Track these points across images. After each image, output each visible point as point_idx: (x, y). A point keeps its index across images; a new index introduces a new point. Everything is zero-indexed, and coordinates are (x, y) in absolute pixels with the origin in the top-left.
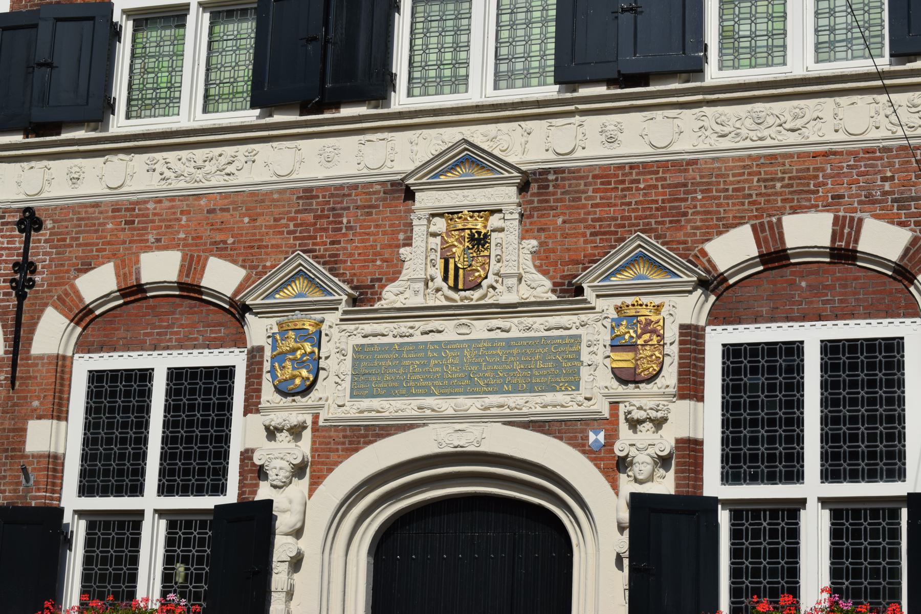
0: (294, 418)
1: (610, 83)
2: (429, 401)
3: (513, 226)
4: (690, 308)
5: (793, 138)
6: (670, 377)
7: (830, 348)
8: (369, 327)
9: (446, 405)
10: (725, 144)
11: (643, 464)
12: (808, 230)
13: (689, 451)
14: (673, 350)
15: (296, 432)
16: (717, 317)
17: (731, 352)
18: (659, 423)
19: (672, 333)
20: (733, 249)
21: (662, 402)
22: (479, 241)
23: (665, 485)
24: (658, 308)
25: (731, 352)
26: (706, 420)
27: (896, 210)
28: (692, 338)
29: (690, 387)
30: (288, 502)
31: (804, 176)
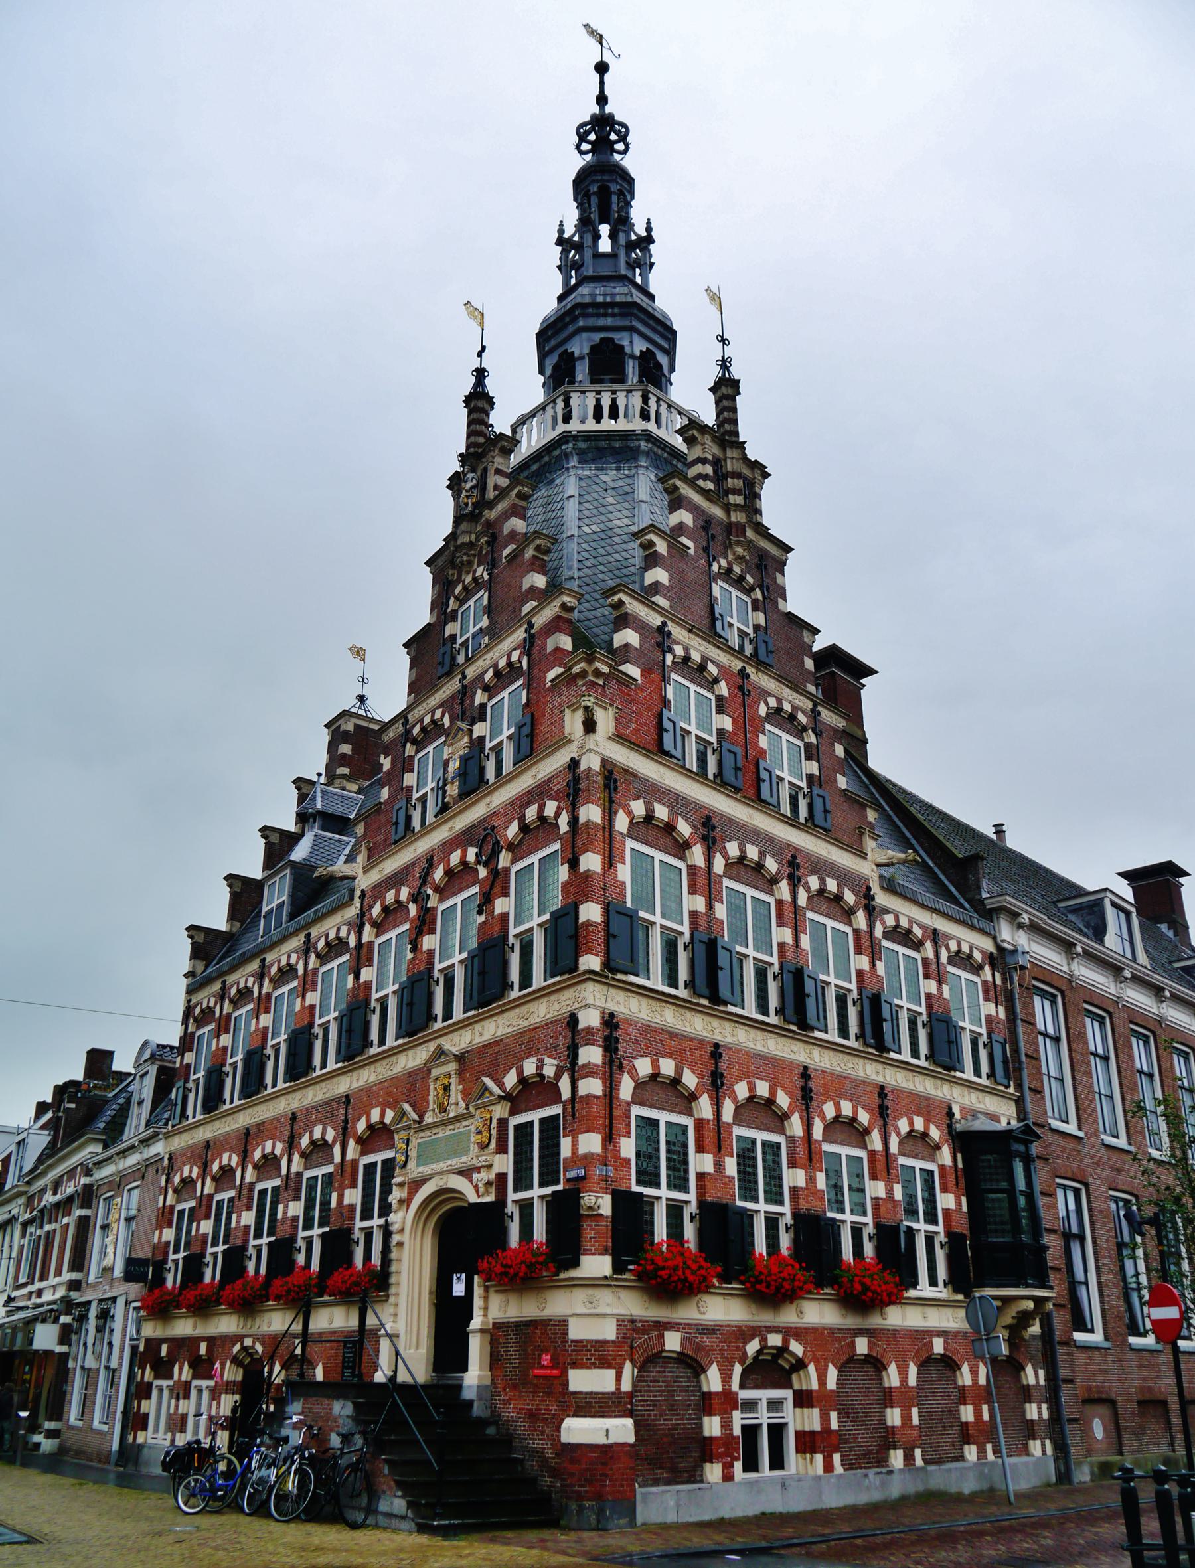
1: (475, 1009)
2: (434, 1166)
3: (454, 1080)
5: (526, 1023)
6: (493, 1145)
8: (421, 1135)
10: (510, 1030)
14: (494, 1132)
16: (513, 1112)
18: (490, 1166)
20: (511, 1080)
21: (489, 1158)
22: (447, 1089)
23: (490, 1198)
24: (490, 1112)
26: (505, 1164)
27: (552, 1051)
28: (503, 1123)
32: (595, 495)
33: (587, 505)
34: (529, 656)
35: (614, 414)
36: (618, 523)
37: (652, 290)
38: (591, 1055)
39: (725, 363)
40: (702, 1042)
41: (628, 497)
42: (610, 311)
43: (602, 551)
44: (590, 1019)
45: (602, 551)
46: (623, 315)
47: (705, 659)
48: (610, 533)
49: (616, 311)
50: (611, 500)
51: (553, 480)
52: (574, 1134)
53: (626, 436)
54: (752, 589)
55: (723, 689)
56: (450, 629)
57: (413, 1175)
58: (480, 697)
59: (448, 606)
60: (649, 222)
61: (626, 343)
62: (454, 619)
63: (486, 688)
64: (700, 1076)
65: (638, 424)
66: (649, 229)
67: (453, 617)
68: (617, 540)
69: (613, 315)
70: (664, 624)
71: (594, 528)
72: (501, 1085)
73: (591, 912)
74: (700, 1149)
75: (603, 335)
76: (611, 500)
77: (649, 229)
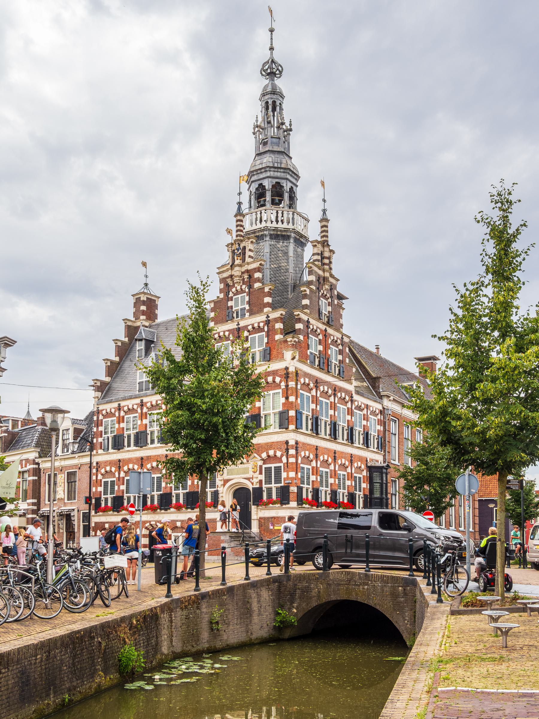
0: (221, 479)
4: (260, 463)
7: (275, 467)
9: (237, 476)
11: (255, 484)
12: (271, 453)
13: (261, 482)
14: (258, 469)
15: (221, 480)
16: (264, 464)
17: (265, 468)
19: (258, 466)
20: (264, 455)
23: (258, 486)
25: (265, 468)
26: (262, 477)
27: (280, 449)
28: (261, 467)
29: (261, 473)
30: (220, 489)
31: (271, 445)
32: (275, 252)
33: (272, 256)
34: (268, 327)
35: (282, 222)
36: (283, 264)
37: (291, 155)
38: (292, 452)
39: (324, 211)
40: (314, 446)
41: (286, 254)
42: (279, 170)
43: (277, 275)
44: (292, 443)
45: (277, 275)
46: (284, 172)
47: (317, 327)
48: (280, 268)
49: (282, 170)
50: (280, 255)
51: (260, 243)
52: (288, 472)
53: (287, 230)
54: (328, 298)
55: (321, 337)
56: (230, 303)
57: (225, 478)
58: (246, 334)
59: (229, 294)
60: (290, 122)
61: (284, 185)
62: (232, 300)
63: (249, 331)
64: (313, 455)
65: (290, 226)
66: (290, 125)
67: (231, 299)
68: (282, 271)
69: (280, 172)
70: (308, 319)
71: (275, 265)
72: (261, 457)
73: (292, 413)
74: (313, 474)
75: (277, 180)
76: (280, 255)
77: (290, 125)
